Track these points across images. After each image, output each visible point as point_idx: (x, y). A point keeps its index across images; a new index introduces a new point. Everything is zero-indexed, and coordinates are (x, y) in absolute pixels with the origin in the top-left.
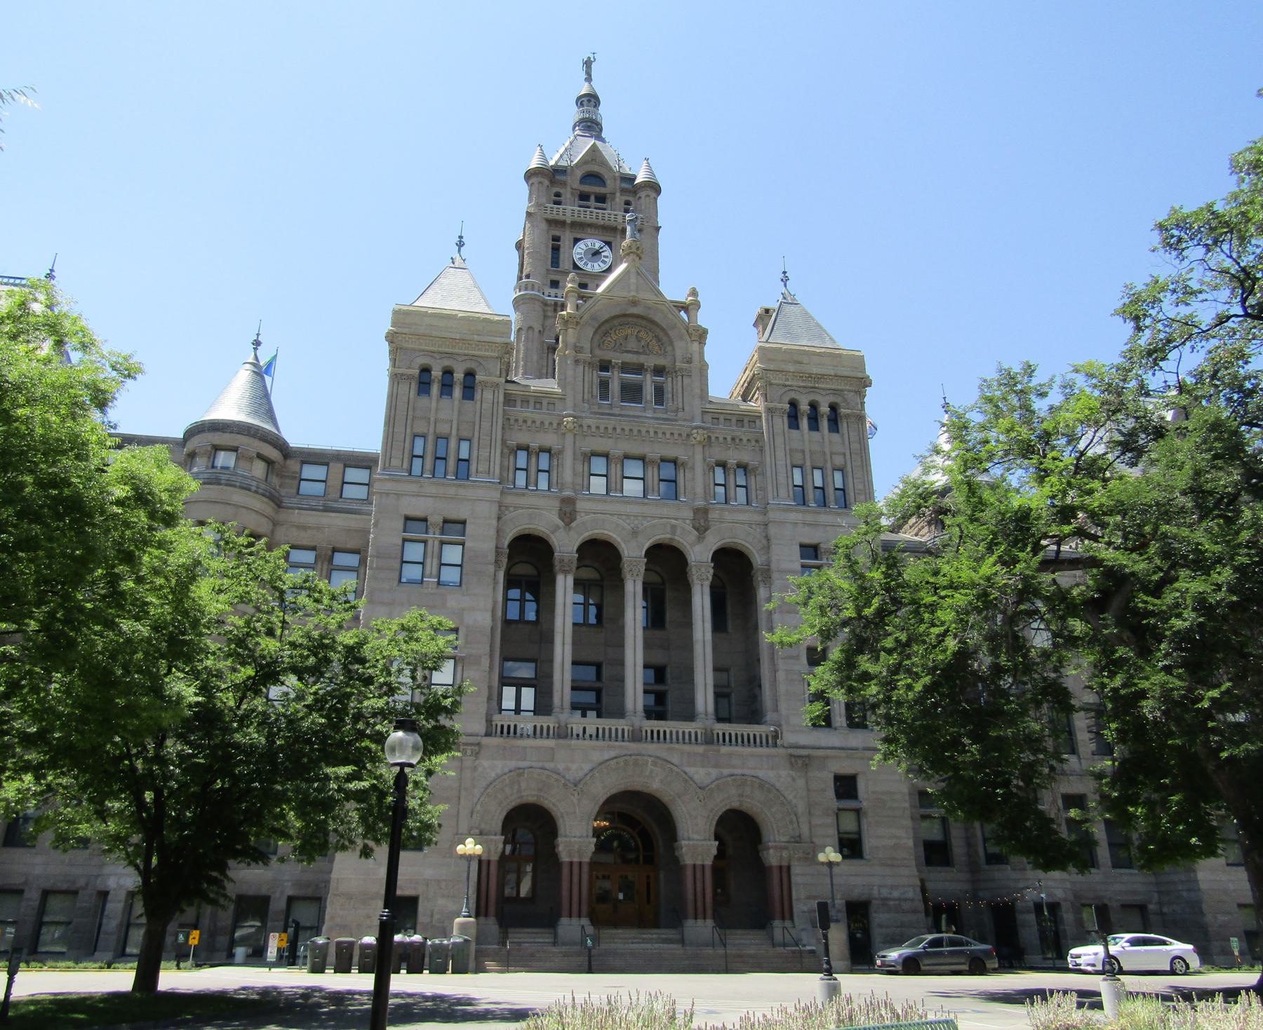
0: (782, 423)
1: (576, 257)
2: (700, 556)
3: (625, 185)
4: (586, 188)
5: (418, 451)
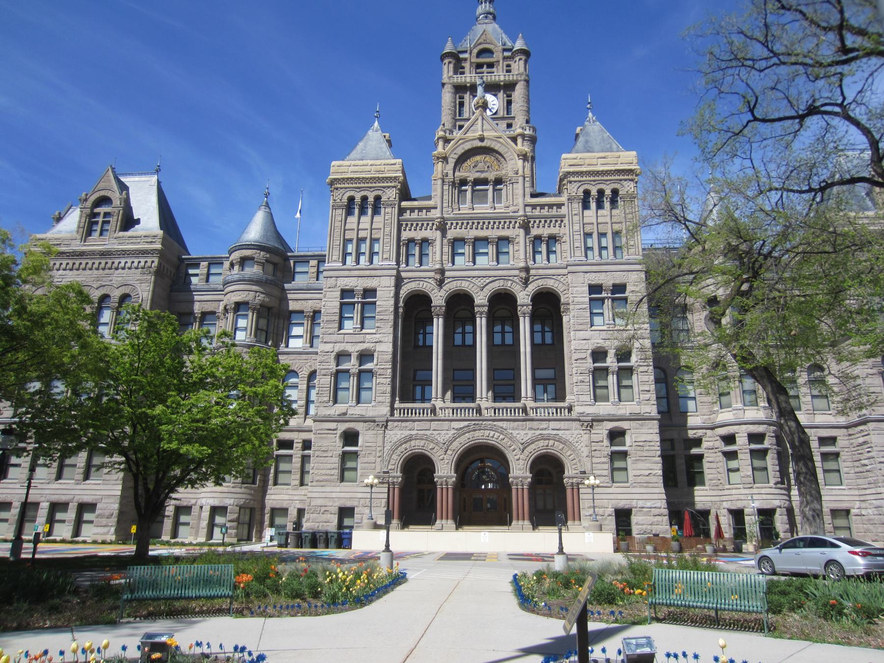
0: (577, 206)
2: (524, 297)
3: (507, 54)
4: (481, 60)
5: (349, 251)
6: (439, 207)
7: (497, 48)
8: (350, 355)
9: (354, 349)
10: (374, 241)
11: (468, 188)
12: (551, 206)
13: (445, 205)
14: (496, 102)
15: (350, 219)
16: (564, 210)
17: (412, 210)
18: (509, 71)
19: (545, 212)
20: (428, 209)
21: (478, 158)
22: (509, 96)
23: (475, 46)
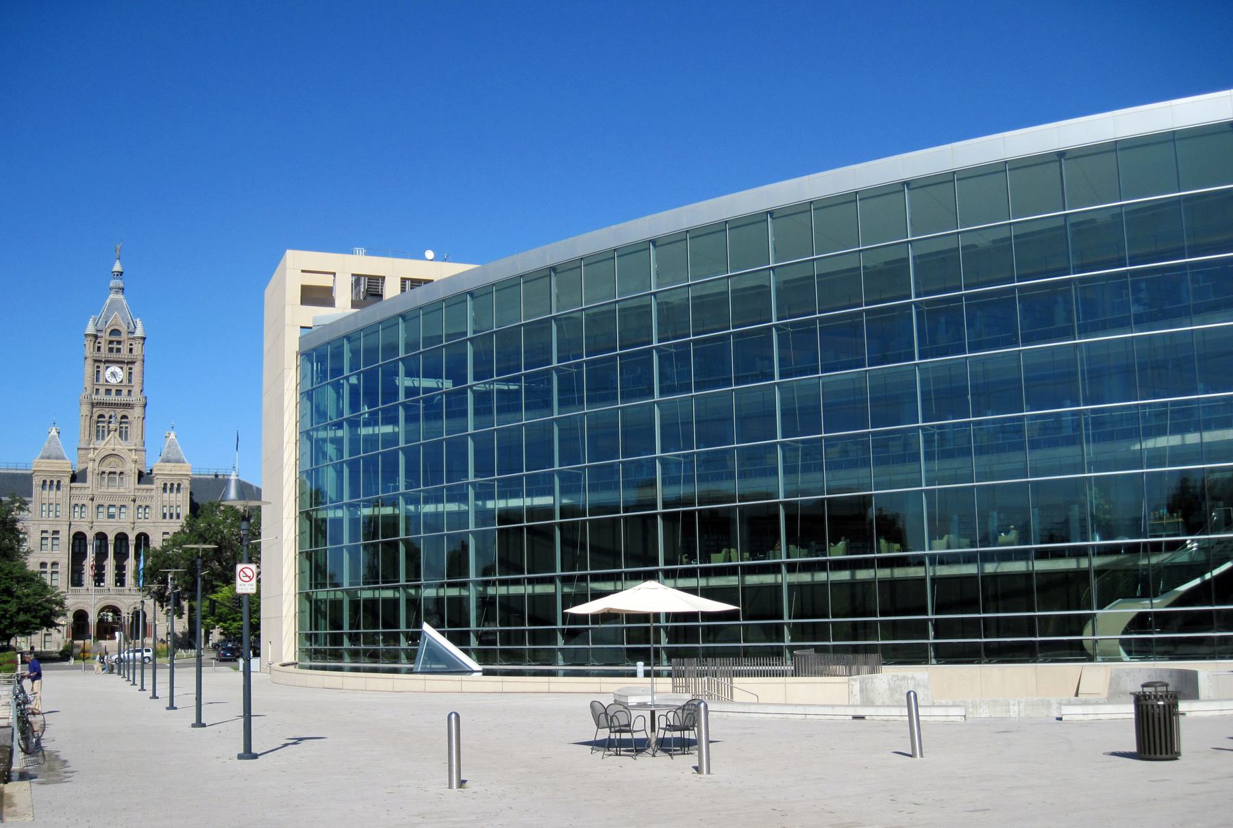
0: (160, 491)
1: (107, 376)
4: (113, 338)
5: (44, 509)
6: (91, 487)
7: (123, 329)
8: (47, 564)
9: (49, 562)
10: (57, 504)
11: (106, 476)
12: (147, 490)
13: (94, 489)
14: (121, 373)
15: (44, 492)
16: (153, 493)
17: (77, 488)
18: (131, 350)
19: (145, 493)
20: (85, 488)
21: (111, 459)
22: (130, 369)
23: (108, 328)
